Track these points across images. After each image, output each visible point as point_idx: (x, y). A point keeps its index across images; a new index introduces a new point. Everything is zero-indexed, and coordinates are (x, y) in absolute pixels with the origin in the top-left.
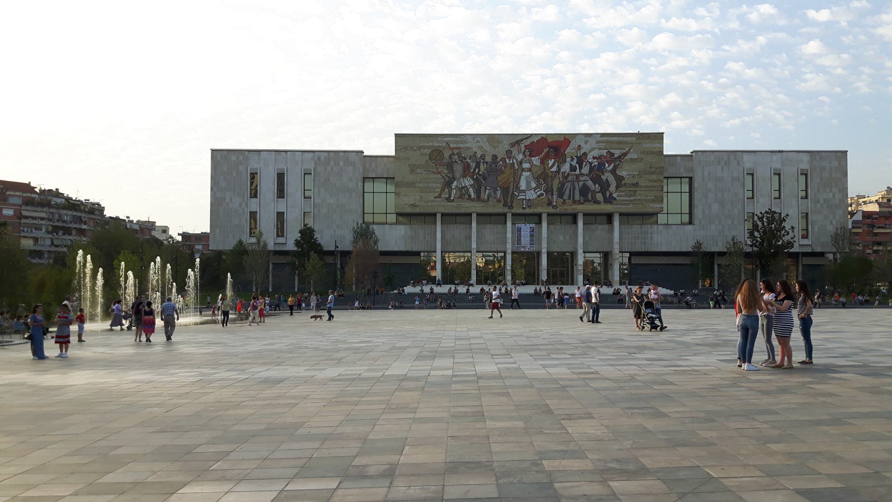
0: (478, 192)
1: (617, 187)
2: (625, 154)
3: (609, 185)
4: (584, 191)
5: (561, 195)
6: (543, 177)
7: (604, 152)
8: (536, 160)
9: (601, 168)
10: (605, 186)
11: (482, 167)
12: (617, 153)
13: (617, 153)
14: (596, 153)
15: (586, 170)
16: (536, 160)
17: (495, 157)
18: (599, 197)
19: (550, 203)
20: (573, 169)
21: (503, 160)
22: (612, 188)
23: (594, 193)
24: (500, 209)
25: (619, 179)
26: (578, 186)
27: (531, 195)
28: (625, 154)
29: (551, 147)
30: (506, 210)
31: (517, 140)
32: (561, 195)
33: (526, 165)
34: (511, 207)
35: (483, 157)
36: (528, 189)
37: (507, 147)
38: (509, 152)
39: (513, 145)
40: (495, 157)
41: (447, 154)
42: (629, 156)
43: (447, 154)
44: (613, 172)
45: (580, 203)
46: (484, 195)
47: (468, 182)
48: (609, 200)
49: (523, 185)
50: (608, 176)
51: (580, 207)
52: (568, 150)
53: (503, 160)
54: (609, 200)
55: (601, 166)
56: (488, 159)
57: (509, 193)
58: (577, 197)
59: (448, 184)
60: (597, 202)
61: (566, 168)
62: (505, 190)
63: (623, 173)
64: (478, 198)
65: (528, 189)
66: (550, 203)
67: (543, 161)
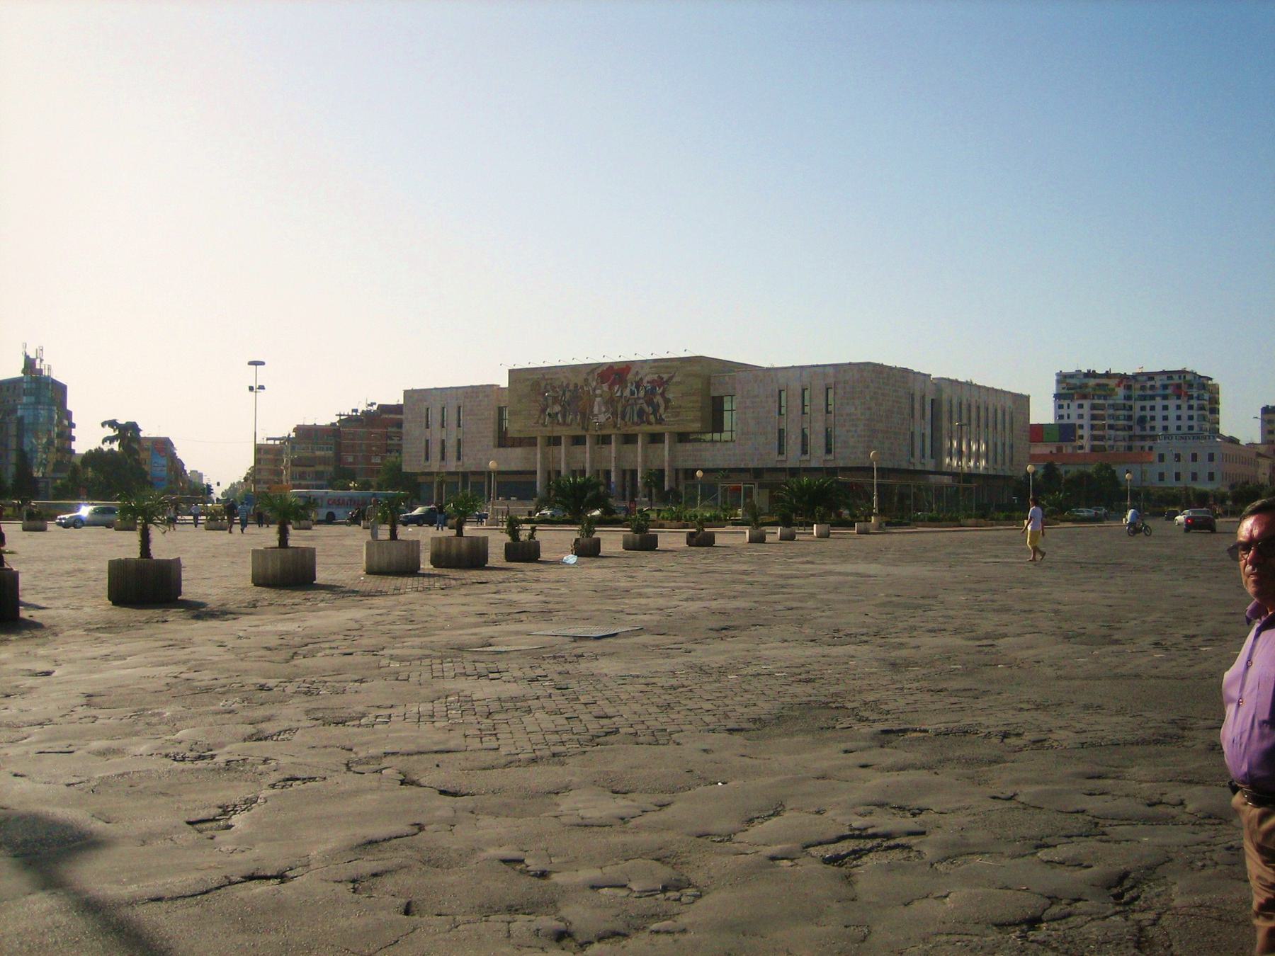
0: (564, 417)
1: (666, 408)
2: (671, 378)
3: (659, 406)
4: (641, 413)
5: (623, 418)
6: (610, 401)
7: (656, 377)
8: (605, 387)
9: (653, 391)
10: (656, 408)
11: (568, 394)
12: (665, 377)
13: (665, 377)
14: (649, 378)
15: (642, 393)
16: (605, 387)
17: (576, 385)
18: (652, 418)
19: (615, 426)
20: (632, 393)
21: (582, 388)
22: (662, 410)
23: (648, 415)
24: (579, 432)
25: (667, 401)
26: (636, 408)
27: (602, 418)
28: (671, 378)
29: (615, 374)
30: (583, 433)
31: (592, 369)
32: (623, 418)
33: (598, 392)
34: (587, 430)
35: (568, 385)
36: (600, 414)
37: (585, 376)
38: (586, 380)
39: (588, 374)
40: (576, 385)
41: (543, 384)
42: (674, 380)
43: (543, 384)
44: (662, 395)
45: (638, 424)
46: (569, 420)
47: (557, 408)
48: (660, 421)
49: (596, 410)
50: (658, 399)
51: (637, 428)
52: (630, 376)
53: (582, 388)
54: (660, 421)
55: (653, 389)
56: (571, 387)
57: (586, 416)
58: (636, 418)
59: (543, 411)
60: (649, 423)
61: (627, 393)
62: (584, 415)
63: (670, 396)
64: (564, 423)
65: (600, 414)
66: (615, 426)
67: (610, 388)
